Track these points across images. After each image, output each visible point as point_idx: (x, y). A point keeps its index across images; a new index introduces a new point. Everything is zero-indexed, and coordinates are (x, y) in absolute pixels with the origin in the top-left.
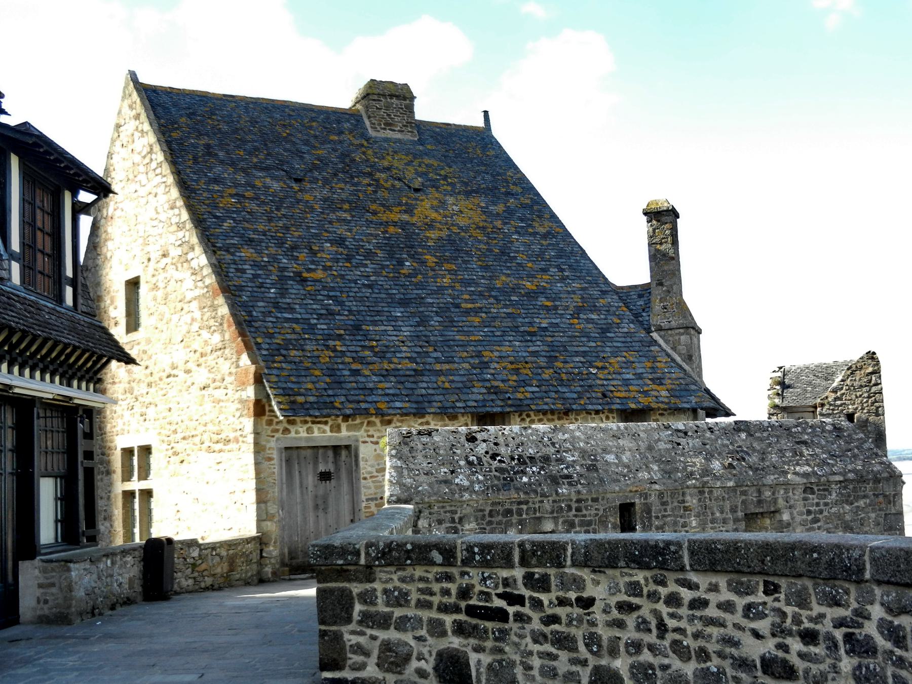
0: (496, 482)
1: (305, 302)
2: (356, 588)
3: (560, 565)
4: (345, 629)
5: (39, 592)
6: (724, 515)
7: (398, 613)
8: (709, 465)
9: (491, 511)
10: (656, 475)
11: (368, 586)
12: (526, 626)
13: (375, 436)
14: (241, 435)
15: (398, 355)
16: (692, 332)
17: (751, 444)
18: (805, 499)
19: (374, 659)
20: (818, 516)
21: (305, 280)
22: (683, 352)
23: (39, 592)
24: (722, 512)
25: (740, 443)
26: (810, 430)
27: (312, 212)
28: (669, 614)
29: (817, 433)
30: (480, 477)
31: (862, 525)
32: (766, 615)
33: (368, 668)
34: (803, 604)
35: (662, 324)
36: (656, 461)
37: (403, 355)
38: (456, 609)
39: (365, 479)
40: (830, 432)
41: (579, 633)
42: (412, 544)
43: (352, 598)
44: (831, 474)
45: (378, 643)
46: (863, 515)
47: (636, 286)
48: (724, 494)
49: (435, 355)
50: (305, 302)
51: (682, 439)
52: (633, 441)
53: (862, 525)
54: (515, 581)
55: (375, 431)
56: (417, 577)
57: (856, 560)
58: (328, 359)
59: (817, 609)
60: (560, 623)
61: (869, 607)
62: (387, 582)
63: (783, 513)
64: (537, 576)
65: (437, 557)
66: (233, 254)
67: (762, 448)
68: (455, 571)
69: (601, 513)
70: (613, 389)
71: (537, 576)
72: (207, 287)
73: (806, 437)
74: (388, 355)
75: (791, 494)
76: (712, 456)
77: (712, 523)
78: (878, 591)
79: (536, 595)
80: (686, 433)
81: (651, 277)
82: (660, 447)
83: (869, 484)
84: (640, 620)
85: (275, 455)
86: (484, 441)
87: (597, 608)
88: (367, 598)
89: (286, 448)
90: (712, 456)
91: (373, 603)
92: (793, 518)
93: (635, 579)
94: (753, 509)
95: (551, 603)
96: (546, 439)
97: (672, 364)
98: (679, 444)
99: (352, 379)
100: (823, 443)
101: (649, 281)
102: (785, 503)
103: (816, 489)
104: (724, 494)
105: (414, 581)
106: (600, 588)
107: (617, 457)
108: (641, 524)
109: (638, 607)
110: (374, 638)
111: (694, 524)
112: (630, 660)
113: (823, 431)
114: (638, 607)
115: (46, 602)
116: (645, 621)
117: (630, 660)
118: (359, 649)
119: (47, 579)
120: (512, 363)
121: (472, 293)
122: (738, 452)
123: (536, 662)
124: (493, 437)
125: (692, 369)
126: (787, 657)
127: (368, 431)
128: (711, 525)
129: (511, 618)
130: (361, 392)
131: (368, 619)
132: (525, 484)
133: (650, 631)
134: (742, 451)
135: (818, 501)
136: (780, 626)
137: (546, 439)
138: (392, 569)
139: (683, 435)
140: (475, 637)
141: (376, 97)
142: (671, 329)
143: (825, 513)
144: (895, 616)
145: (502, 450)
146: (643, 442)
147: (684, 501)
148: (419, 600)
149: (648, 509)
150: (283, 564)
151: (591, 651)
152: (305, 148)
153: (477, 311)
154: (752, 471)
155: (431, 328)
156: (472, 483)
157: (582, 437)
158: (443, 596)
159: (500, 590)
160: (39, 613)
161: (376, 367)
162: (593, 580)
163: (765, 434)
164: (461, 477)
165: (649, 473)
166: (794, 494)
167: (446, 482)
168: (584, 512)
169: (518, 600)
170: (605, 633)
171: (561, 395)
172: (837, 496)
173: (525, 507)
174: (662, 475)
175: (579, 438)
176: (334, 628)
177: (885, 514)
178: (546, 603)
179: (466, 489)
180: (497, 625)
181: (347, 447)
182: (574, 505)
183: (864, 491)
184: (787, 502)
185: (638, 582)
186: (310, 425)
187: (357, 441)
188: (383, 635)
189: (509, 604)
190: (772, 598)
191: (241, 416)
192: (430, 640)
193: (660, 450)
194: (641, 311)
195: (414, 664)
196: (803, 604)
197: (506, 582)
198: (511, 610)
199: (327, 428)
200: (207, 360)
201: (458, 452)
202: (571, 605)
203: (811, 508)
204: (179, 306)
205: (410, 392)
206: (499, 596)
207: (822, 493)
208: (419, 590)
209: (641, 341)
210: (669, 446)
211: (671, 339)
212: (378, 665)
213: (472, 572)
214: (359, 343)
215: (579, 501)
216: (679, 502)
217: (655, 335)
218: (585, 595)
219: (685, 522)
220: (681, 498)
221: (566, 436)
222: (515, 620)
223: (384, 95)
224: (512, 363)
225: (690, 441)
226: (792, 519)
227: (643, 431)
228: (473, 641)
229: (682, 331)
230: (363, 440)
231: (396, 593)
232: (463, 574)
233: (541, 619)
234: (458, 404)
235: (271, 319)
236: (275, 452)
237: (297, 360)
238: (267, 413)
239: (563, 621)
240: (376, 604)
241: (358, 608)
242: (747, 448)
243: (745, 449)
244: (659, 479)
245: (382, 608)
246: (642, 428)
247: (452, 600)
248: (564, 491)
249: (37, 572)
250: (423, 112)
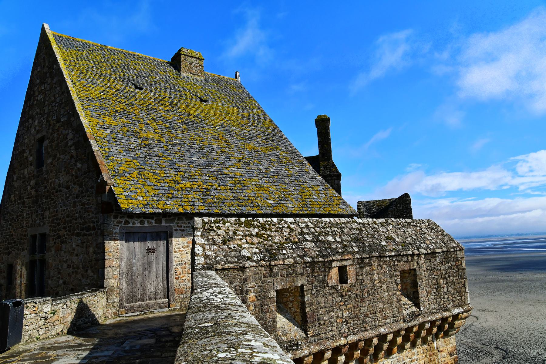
13: (182, 226)
39: (176, 252)
55: (182, 223)
127: (179, 223)
157: (312, 226)
186: (142, 219)
187: (172, 229)
199: (153, 221)
200: (79, 180)
230: (175, 228)
236: (119, 235)
238: (114, 211)
248: (309, 259)
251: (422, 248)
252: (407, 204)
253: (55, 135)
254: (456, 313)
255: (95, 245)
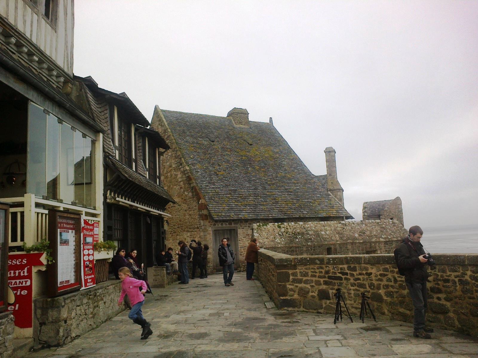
0: (288, 241)
1: (218, 182)
2: (290, 272)
3: (360, 264)
4: (287, 283)
5: (154, 278)
7: (304, 279)
9: (287, 251)
11: (295, 271)
12: (349, 281)
14: (200, 226)
15: (249, 199)
18: (385, 246)
19: (297, 293)
21: (217, 175)
23: (154, 278)
24: (359, 251)
27: (218, 152)
28: (398, 276)
30: (283, 240)
32: (432, 276)
33: (295, 295)
34: (444, 271)
37: (250, 199)
38: (325, 277)
39: (240, 240)
41: (366, 283)
42: (309, 258)
43: (289, 274)
45: (298, 288)
49: (261, 199)
50: (218, 182)
54: (344, 268)
56: (311, 268)
57: (462, 259)
58: (227, 201)
59: (449, 273)
60: (360, 280)
61: (466, 272)
62: (301, 269)
64: (352, 267)
65: (318, 262)
66: (194, 166)
68: (324, 266)
69: (321, 251)
70: (318, 210)
71: (352, 267)
72: (187, 177)
74: (246, 199)
78: (470, 268)
79: (351, 272)
84: (388, 278)
85: (211, 233)
86: (283, 228)
87: (373, 275)
88: (294, 274)
89: (215, 230)
91: (296, 276)
93: (386, 267)
94: (368, 250)
95: (357, 274)
96: (302, 227)
98: (344, 228)
99: (235, 207)
100: (389, 227)
105: (310, 269)
106: (373, 270)
107: (325, 233)
109: (387, 275)
110: (297, 286)
112: (385, 291)
114: (387, 275)
115: (156, 280)
116: (389, 279)
117: (385, 291)
118: (292, 290)
119: (156, 273)
120: (285, 202)
121: (271, 178)
123: (352, 292)
124: (286, 226)
126: (439, 287)
129: (343, 279)
130: (239, 212)
131: (294, 281)
132: (297, 241)
133: (391, 281)
136: (436, 278)
137: (302, 227)
138: (303, 266)
140: (331, 285)
141: (236, 114)
144: (475, 274)
145: (289, 230)
148: (312, 275)
150: (214, 269)
151: (371, 289)
152: (214, 131)
153: (273, 184)
155: (259, 190)
156: (281, 241)
158: (320, 273)
159: (339, 271)
160: (154, 284)
161: (243, 203)
162: (371, 267)
163: (371, 225)
164: (277, 239)
167: (273, 241)
168: (316, 251)
169: (347, 274)
170: (376, 283)
171: (302, 212)
173: (298, 249)
175: (312, 226)
176: (283, 283)
178: (355, 274)
179: (279, 243)
180: (338, 281)
181: (234, 230)
182: (313, 249)
185: (387, 268)
187: (237, 228)
188: (300, 285)
189: (342, 275)
190: (433, 271)
191: (200, 220)
192: (316, 287)
195: (311, 294)
196: (444, 271)
197: (341, 269)
198: (343, 277)
199: (228, 223)
201: (276, 231)
202: (364, 275)
204: (176, 183)
205: (254, 211)
206: (339, 273)
208: (311, 272)
210: (341, 229)
212: (298, 294)
213: (330, 266)
214: (237, 196)
215: (314, 247)
217: (329, 192)
218: (369, 272)
220: (346, 246)
221: (309, 226)
222: (345, 280)
223: (239, 113)
224: (285, 202)
228: (331, 287)
231: (304, 273)
232: (326, 267)
233: (354, 279)
234: (270, 215)
235: (208, 188)
237: (218, 201)
239: (361, 280)
240: (297, 276)
241: (291, 277)
245: (299, 277)
247: (323, 274)
249: (153, 271)
250: (251, 118)
253: (169, 174)
255: (199, 237)
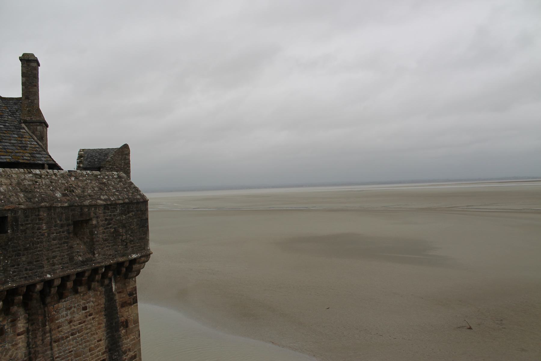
6: (62, 222)
8: (54, 195)
10: (22, 200)
16: (44, 125)
17: (77, 183)
18: (104, 213)
20: (110, 221)
22: (38, 135)
24: (61, 221)
25: (71, 183)
26: (107, 177)
29: (110, 179)
31: (130, 225)
35: (27, 119)
36: (22, 191)
40: (116, 178)
44: (117, 200)
46: (131, 220)
47: (13, 98)
48: (62, 211)
51: (38, 179)
52: (8, 179)
53: (130, 225)
63: (93, 220)
67: (83, 186)
73: (105, 180)
75: (97, 210)
76: (56, 189)
77: (55, 227)
80: (41, 176)
81: (22, 94)
82: (25, 183)
83: (134, 205)
90: (56, 189)
92: (98, 223)
97: (32, 140)
100: (113, 184)
101: (21, 96)
102: (95, 215)
103: (110, 207)
104: (62, 211)
108: (11, 229)
111: (44, 227)
113: (113, 178)
122: (70, 187)
125: (43, 144)
128: (54, 228)
134: (73, 187)
135: (111, 213)
139: (39, 177)
142: (32, 123)
143: (114, 220)
146: (15, 180)
147: (39, 215)
149: (16, 220)
154: (78, 197)
163: (84, 178)
165: (18, 198)
166: (99, 210)
172: (119, 211)
174: (26, 200)
177: (141, 220)
183: (132, 208)
184: (95, 214)
193: (25, 185)
194: (15, 111)
203: (107, 217)
207: (112, 209)
209: (15, 126)
210: (31, 183)
211: (32, 127)
216: (36, 216)
217: (23, 125)
219: (39, 227)
220: (37, 213)
225: (43, 180)
226: (98, 223)
227: (15, 173)
229: (38, 124)
242: (75, 185)
243: (74, 186)
244: (24, 202)
246: (14, 172)
251: (101, 200)
252: (126, 154)
254: (132, 258)
